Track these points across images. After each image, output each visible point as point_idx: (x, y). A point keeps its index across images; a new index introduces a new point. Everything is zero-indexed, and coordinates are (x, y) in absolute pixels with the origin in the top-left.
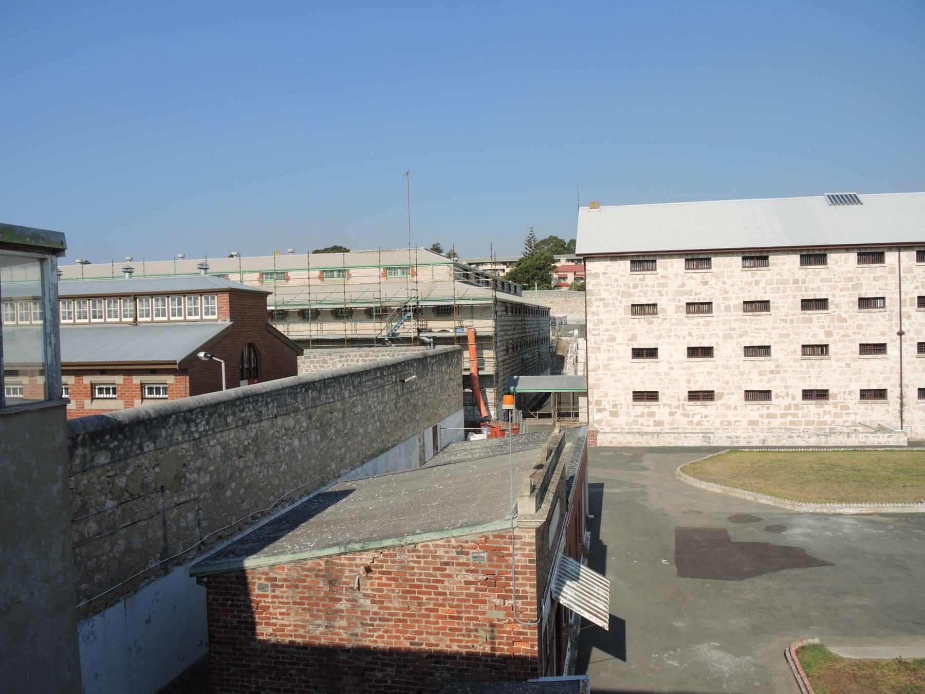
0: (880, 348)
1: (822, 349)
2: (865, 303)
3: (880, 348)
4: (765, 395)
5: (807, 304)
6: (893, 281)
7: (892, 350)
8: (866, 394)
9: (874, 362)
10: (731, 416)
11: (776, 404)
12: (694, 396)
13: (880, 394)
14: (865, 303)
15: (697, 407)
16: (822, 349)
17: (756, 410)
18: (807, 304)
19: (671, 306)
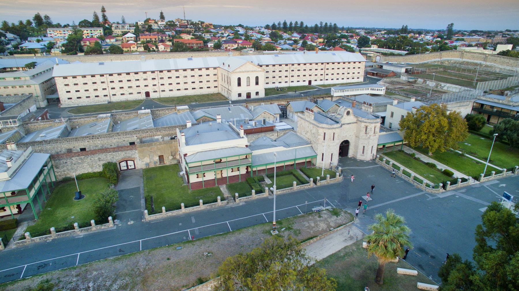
0: (105, 89)
1: (97, 90)
2: (102, 82)
3: (105, 89)
4: (89, 97)
5: (93, 83)
6: (106, 79)
7: (107, 89)
8: (105, 96)
9: (105, 91)
10: (84, 100)
11: (91, 98)
12: (78, 98)
13: (107, 96)
14: (102, 82)
15: (79, 99)
16: (97, 90)
17: (88, 99)
18: (93, 83)
19: (71, 84)
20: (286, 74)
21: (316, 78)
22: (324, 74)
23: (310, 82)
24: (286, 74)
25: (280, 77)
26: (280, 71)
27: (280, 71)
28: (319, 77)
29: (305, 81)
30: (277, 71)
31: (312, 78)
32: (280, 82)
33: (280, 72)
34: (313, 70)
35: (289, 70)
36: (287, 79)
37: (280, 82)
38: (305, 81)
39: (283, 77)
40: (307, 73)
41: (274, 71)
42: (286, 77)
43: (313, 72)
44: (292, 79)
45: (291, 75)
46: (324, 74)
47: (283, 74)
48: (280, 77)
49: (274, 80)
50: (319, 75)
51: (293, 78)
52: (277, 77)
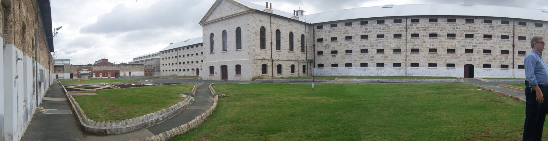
20: (396, 43)
21: (487, 59)
22: (511, 35)
23: (469, 71)
24: (396, 43)
25: (380, 51)
26: (380, 36)
27: (380, 36)
28: (496, 58)
29: (452, 65)
30: (373, 36)
31: (477, 60)
32: (380, 65)
33: (380, 40)
34: (479, 39)
35: (403, 34)
36: (399, 58)
37: (380, 65)
38: (452, 65)
39: (389, 51)
40: (460, 44)
41: (364, 37)
42: (397, 51)
43: (479, 44)
44: (414, 57)
45: (410, 47)
46: (511, 35)
47: (390, 43)
48: (380, 51)
49: (365, 58)
50: (496, 51)
51: (415, 54)
52: (373, 52)
